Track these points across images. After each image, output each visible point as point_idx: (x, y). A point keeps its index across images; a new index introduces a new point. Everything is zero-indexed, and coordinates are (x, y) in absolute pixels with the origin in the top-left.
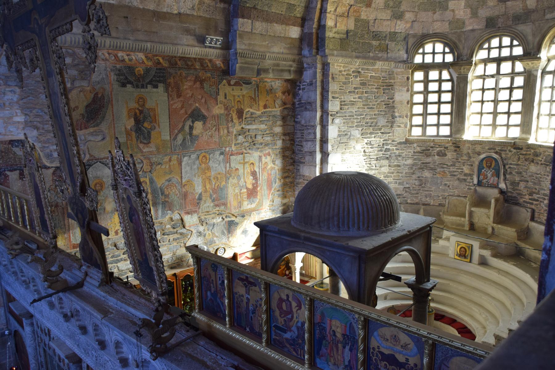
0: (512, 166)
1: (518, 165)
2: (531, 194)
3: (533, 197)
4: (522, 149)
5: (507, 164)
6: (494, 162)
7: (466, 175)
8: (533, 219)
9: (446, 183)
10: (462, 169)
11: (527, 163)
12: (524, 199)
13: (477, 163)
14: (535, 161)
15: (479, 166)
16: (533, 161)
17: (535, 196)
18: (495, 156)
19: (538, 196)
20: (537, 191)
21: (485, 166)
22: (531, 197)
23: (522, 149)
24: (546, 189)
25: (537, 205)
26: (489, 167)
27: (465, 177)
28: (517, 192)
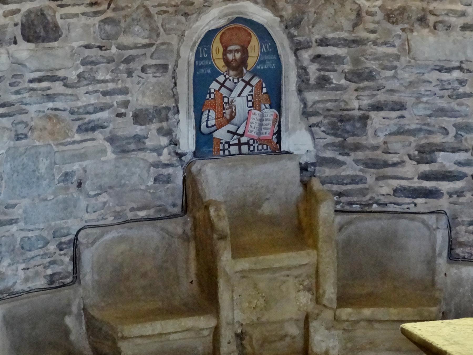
0: (322, 50)
2: (425, 154)
5: (308, 46)
6: (255, 42)
7: (140, 117)
9: (67, 168)
10: (125, 91)
11: (397, 29)
12: (395, 183)
13: (188, 55)
14: (432, 19)
15: (197, 68)
17: (445, 161)
19: (461, 156)
20: (450, 139)
22: (425, 168)
25: (460, 194)
28: (360, 155)
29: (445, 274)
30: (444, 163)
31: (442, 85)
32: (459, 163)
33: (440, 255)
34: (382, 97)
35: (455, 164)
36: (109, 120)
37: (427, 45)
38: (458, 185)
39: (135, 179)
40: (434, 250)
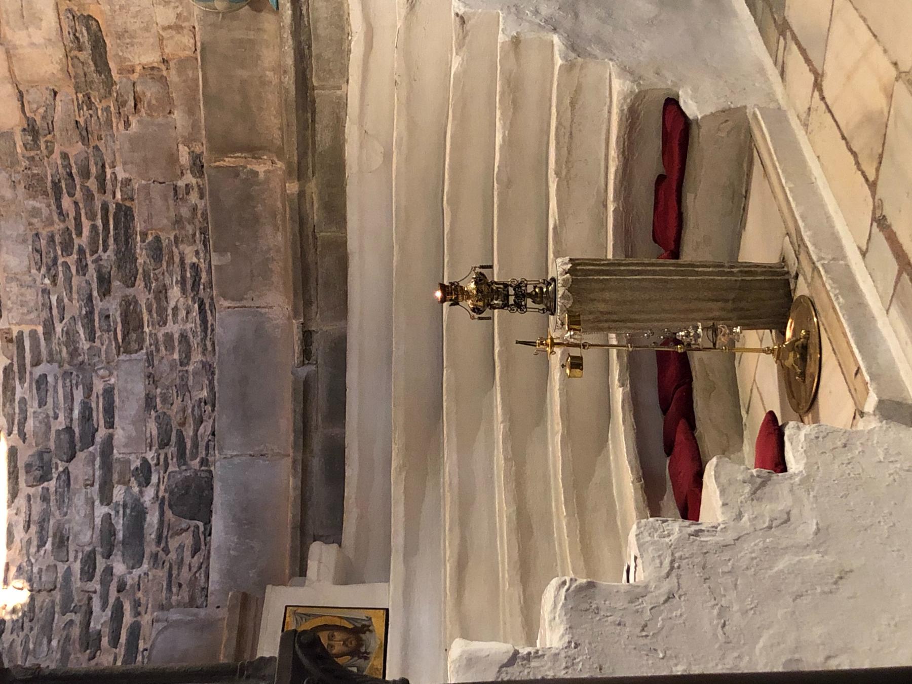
3: (106, 631)
17: (100, 619)
20: (77, 618)
22: (105, 641)
24: (62, 568)
25: (137, 604)
29: (218, 607)
30: (102, 621)
32: (104, 607)
33: (196, 615)
35: (104, 611)
38: (127, 607)
40: (190, 622)
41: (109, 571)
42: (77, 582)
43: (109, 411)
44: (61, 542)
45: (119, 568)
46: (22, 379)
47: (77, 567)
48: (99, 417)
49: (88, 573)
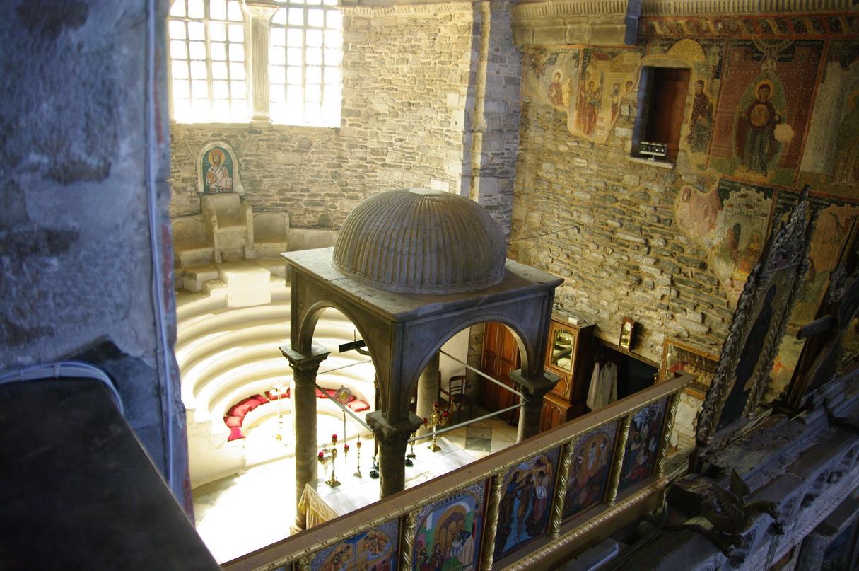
1: (255, 156)
4: (260, 133)
5: (241, 156)
6: (223, 155)
7: (184, 180)
8: (291, 226)
10: (179, 172)
11: (271, 151)
13: (200, 159)
14: (283, 148)
15: (203, 164)
16: (280, 149)
17: (288, 194)
18: (225, 146)
19: (293, 193)
20: (289, 187)
21: (211, 163)
22: (281, 197)
23: (260, 133)
24: (305, 182)
25: (293, 205)
26: (218, 163)
27: (184, 185)
31: (286, 170)
32: (293, 195)
34: (266, 173)
36: (173, 182)
37: (281, 157)
38: (292, 202)
39: (183, 202)
41: (304, 196)
42: (300, 187)
43: (352, 198)
44: (312, 182)
45: (304, 199)
46: (363, 171)
47: (305, 187)
48: (351, 194)
49: (302, 190)
